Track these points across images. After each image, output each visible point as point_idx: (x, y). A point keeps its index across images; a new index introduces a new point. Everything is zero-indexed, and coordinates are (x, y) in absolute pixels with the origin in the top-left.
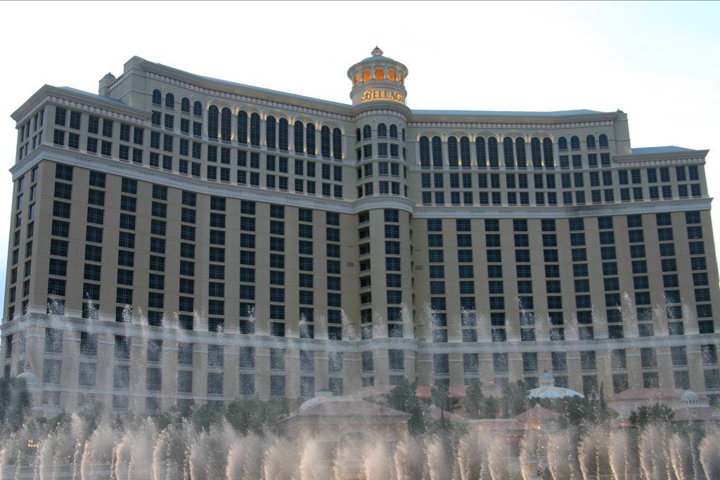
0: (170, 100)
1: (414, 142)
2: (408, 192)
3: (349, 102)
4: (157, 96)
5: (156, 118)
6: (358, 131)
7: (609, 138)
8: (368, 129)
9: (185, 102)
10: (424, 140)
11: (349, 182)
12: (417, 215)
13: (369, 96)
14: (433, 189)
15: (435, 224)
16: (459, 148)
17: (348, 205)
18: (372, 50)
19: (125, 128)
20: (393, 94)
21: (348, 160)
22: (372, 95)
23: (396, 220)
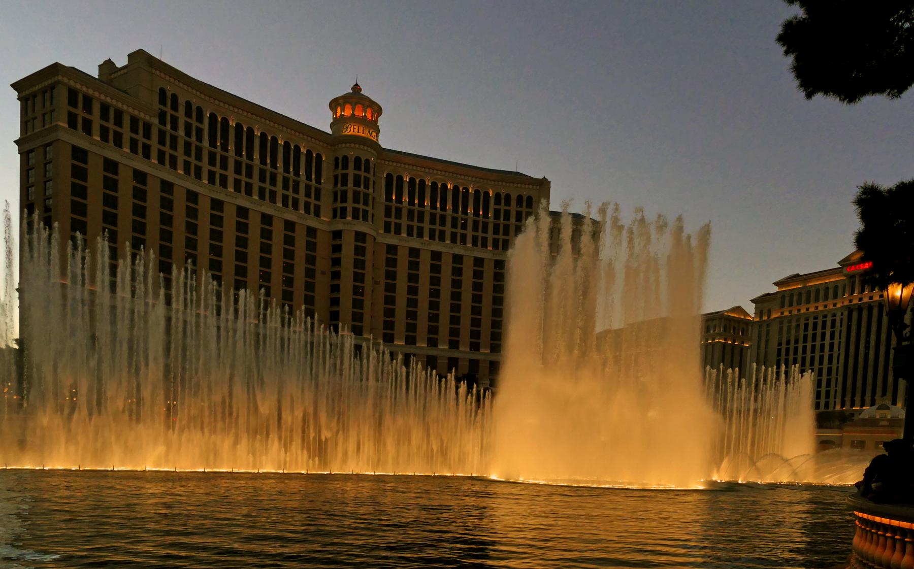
0: (175, 98)
1: (382, 177)
2: (374, 218)
3: (330, 132)
4: (162, 92)
5: (162, 117)
6: (337, 159)
7: (534, 199)
8: (345, 159)
9: (188, 105)
10: (389, 176)
11: (326, 203)
12: (379, 239)
13: (349, 129)
14: (393, 220)
15: (391, 249)
16: (417, 188)
17: (324, 223)
18: (352, 86)
19: (134, 121)
20: (369, 131)
21: (327, 185)
22: (352, 128)
23: (364, 242)
